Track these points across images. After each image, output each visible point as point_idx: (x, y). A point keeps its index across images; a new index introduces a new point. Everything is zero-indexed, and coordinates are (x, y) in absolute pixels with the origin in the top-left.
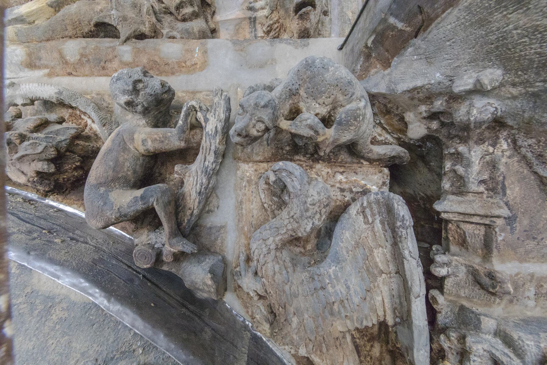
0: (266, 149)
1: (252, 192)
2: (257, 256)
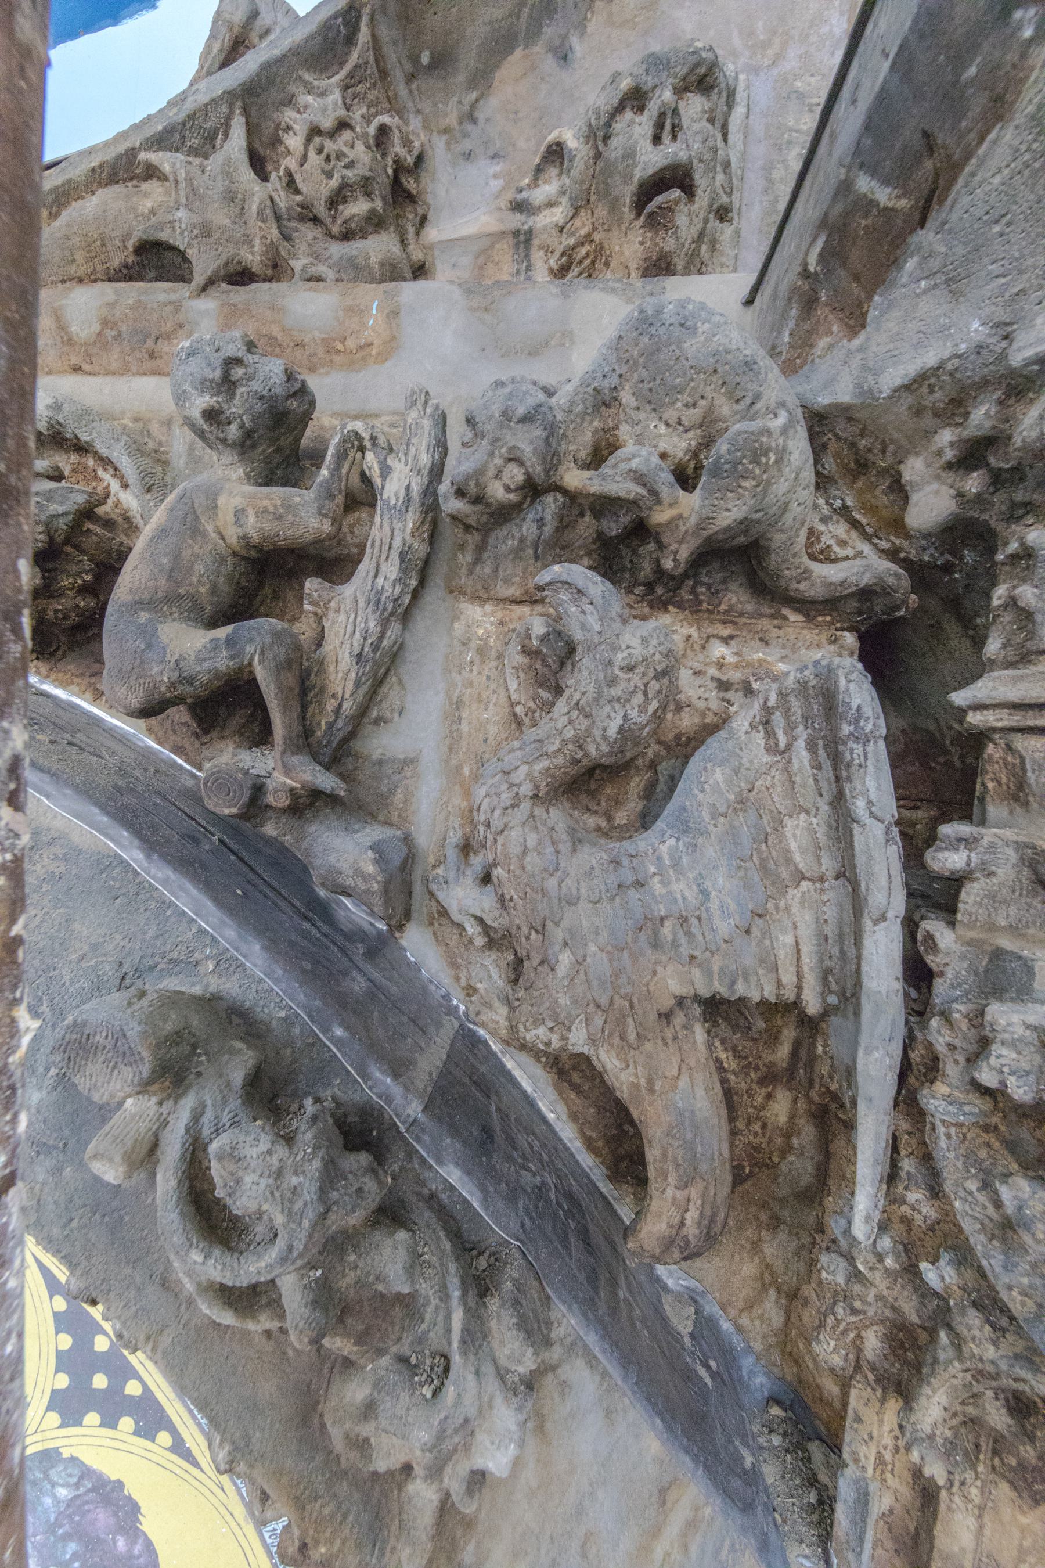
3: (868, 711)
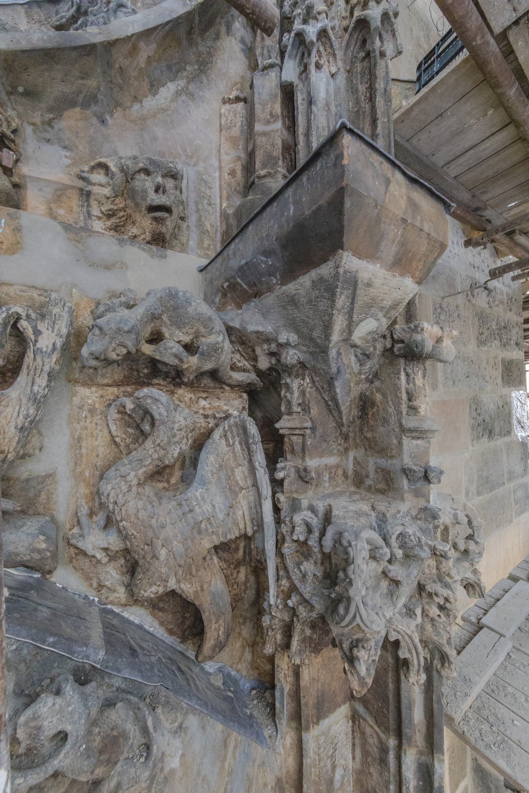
0: (116, 370)
1: (96, 424)
2: (114, 497)
3: (256, 435)
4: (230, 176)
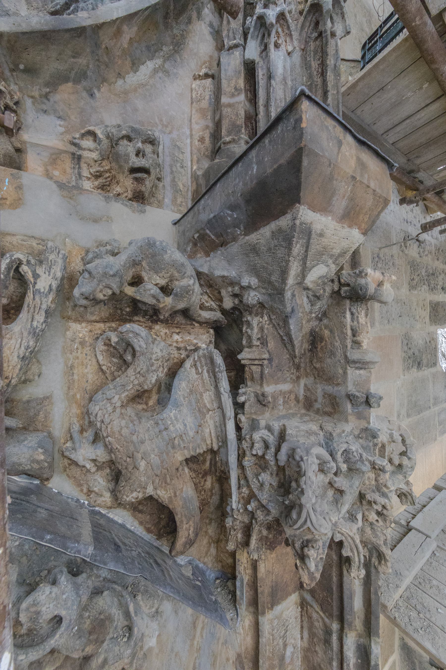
0: (103, 308)
1: (86, 355)
2: (101, 417)
3: (221, 365)
4: (200, 143)
